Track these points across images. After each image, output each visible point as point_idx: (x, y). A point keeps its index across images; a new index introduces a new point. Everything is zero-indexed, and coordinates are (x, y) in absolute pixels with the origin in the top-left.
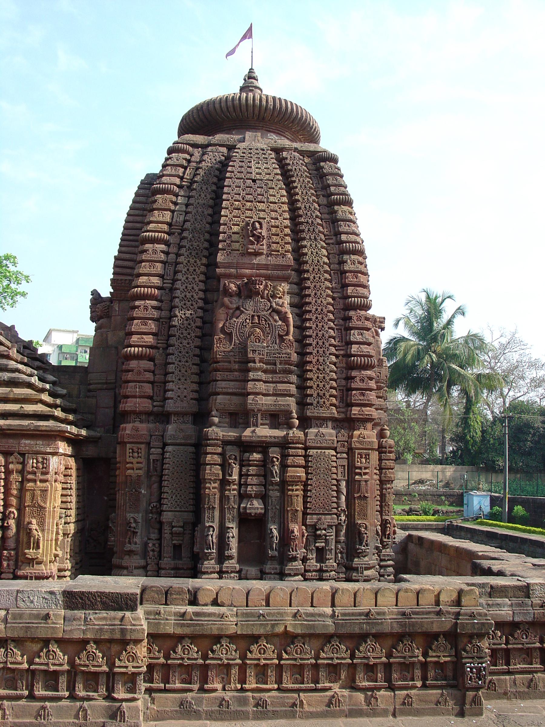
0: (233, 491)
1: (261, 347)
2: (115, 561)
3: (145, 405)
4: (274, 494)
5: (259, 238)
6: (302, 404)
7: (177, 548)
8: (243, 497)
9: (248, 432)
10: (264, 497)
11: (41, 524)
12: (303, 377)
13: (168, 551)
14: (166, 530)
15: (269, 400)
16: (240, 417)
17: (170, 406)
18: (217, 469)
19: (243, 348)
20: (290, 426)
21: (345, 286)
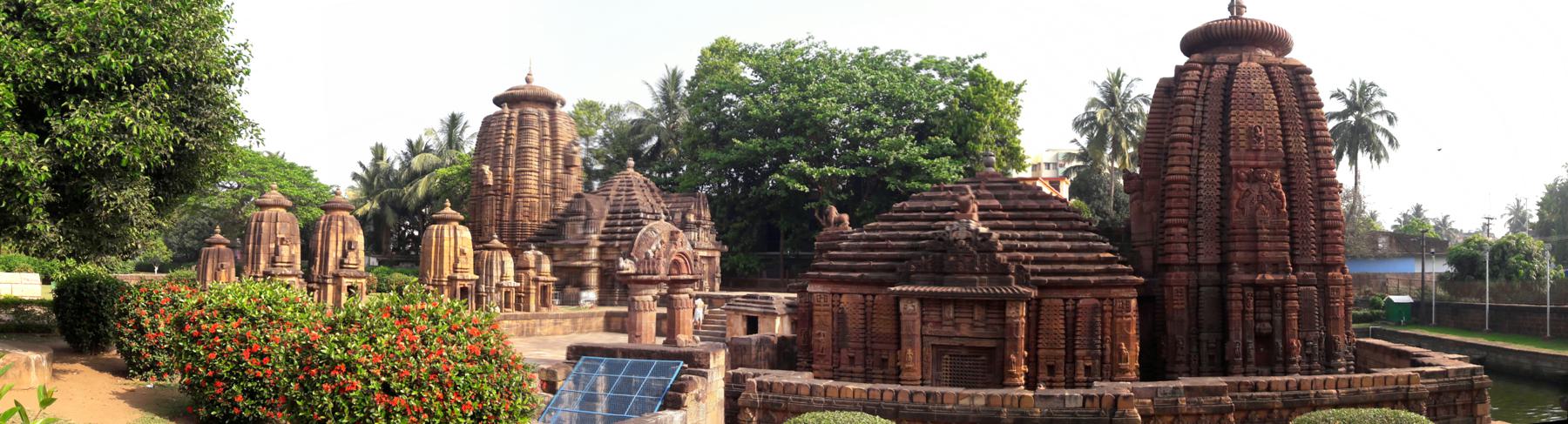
0: (1250, 317)
1: (1266, 216)
2: (1169, 368)
3: (1184, 259)
4: (1278, 318)
5: (1259, 138)
6: (1292, 256)
7: (1211, 357)
8: (1257, 321)
9: (1259, 277)
10: (1271, 321)
11: (1128, 346)
12: (1292, 237)
13: (1205, 360)
14: (1204, 345)
15: (1273, 254)
16: (1254, 266)
17: (1201, 259)
18: (1240, 304)
19: (1253, 217)
20: (1287, 272)
21: (1319, 169)
